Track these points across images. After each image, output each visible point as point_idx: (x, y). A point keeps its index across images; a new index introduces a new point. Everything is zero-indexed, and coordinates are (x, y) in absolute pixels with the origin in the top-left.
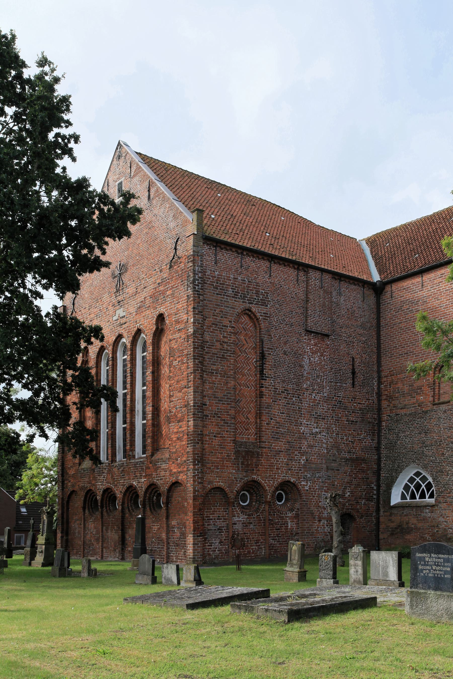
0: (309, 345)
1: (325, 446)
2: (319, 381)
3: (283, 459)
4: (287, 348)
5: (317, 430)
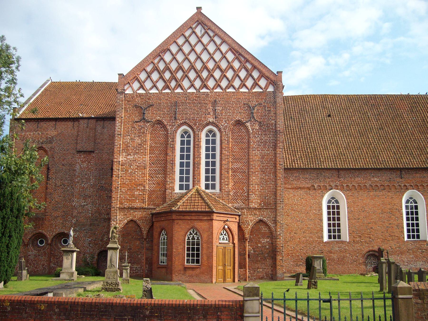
0: (79, 159)
1: (90, 212)
2: (87, 176)
3: (60, 221)
4: (65, 162)
5: (85, 204)
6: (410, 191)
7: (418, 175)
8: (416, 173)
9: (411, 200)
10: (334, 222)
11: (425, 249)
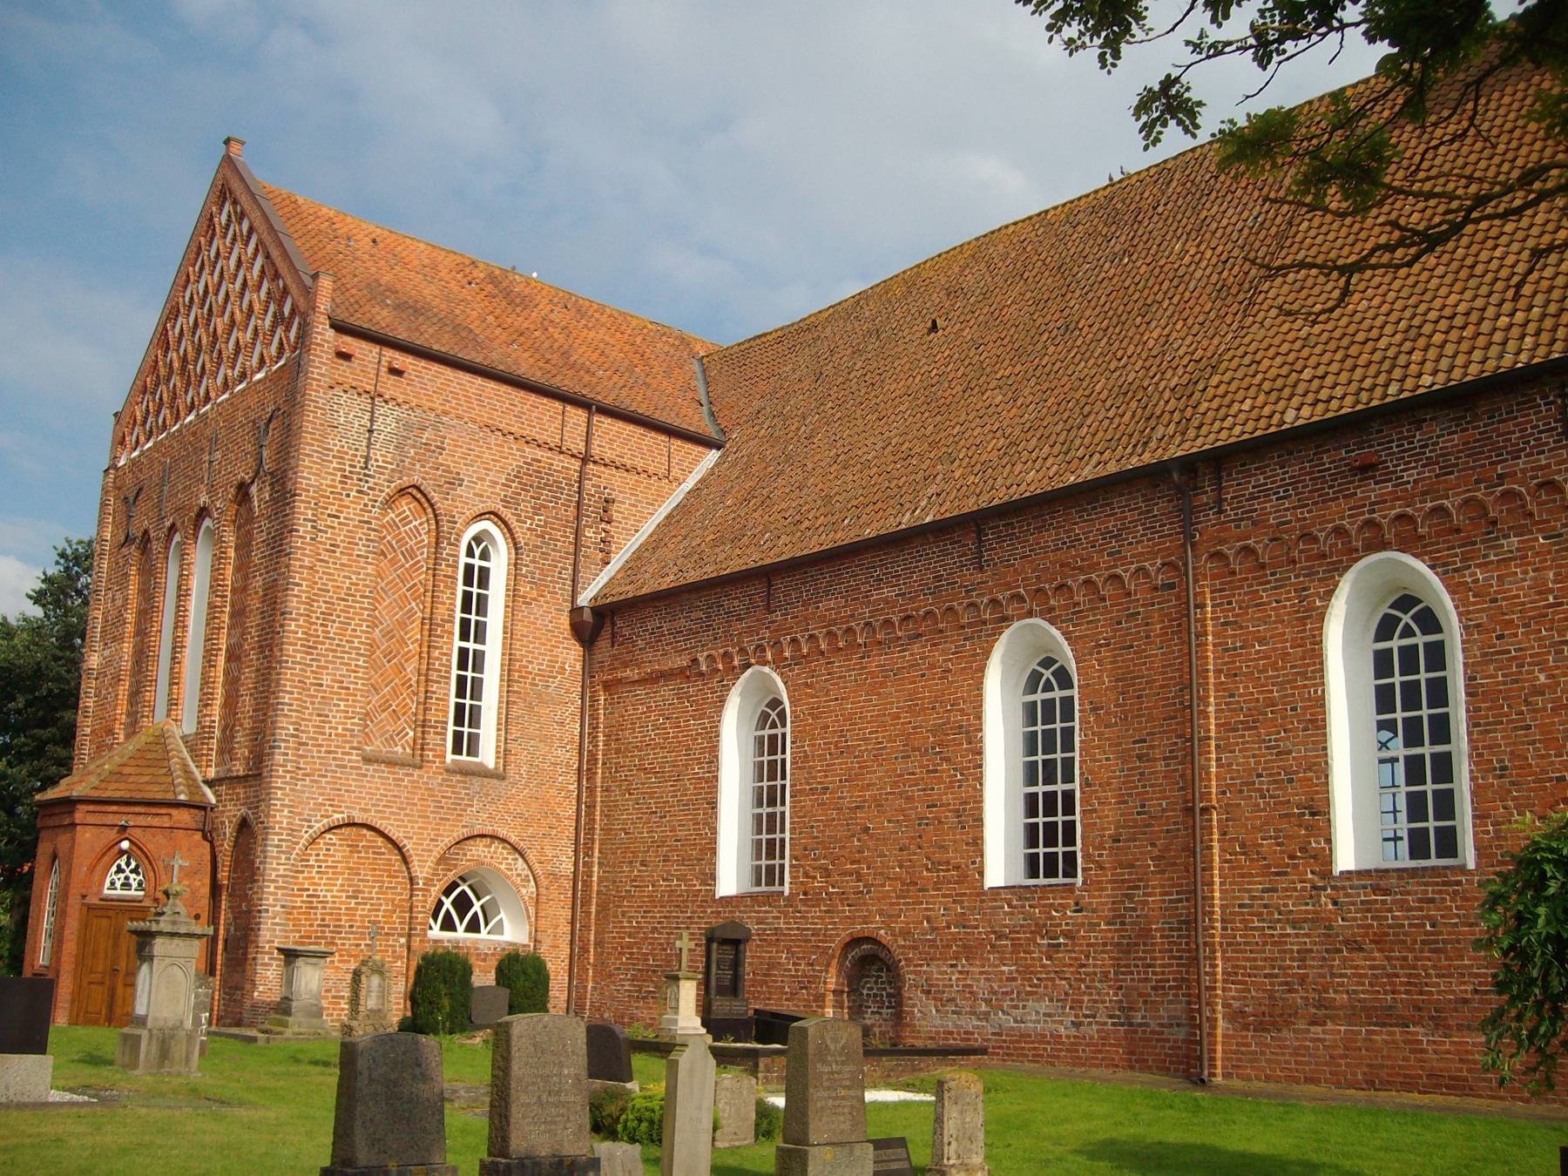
6: (1016, 624)
7: (1049, 537)
8: (1039, 529)
9: (1047, 674)
10: (770, 810)
11: (1066, 934)
